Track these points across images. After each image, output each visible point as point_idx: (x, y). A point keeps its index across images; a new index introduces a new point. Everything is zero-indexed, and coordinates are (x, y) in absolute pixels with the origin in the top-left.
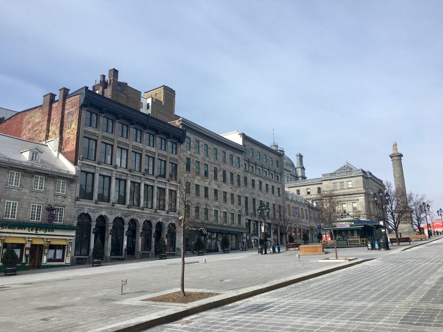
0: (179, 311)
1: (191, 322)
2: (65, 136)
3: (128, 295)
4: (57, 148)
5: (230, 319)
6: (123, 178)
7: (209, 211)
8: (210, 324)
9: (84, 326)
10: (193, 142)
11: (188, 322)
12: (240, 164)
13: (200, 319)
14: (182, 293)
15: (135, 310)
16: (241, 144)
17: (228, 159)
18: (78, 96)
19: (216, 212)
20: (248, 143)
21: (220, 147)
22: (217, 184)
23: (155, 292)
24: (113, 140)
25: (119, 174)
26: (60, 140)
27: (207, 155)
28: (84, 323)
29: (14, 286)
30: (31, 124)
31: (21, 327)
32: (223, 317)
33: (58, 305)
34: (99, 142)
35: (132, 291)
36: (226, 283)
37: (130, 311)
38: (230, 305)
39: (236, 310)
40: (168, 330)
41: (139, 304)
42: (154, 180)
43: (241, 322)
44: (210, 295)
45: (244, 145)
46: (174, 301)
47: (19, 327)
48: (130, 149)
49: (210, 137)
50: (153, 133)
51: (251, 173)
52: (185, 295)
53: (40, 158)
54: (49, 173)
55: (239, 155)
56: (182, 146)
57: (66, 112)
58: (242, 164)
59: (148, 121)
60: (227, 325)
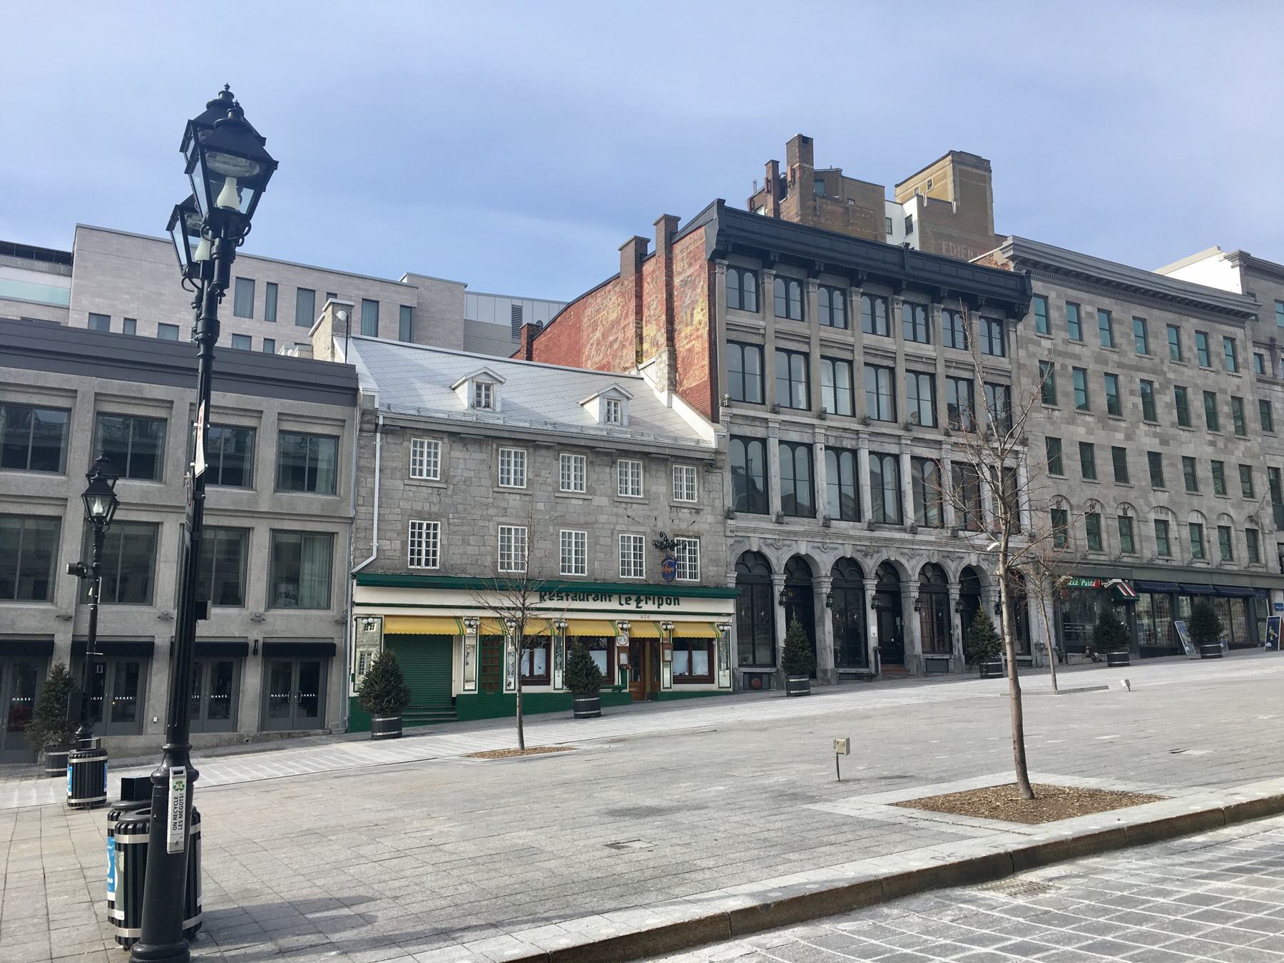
0: (1001, 850)
1: (1043, 889)
2: (682, 345)
3: (857, 787)
4: (666, 383)
5: (1188, 891)
6: (848, 444)
7: (1135, 524)
8: (1112, 902)
9: (708, 874)
10: (1059, 308)
11: (1033, 889)
12: (1240, 360)
13: (1081, 881)
14: (1022, 790)
15: (865, 833)
16: (1240, 292)
17: (1190, 349)
18: (702, 230)
19: (1162, 525)
20: (1263, 285)
21: (1156, 312)
22: (1155, 435)
23: (940, 780)
24: (806, 340)
25: (834, 433)
26: (669, 358)
27: (1113, 345)
28: (711, 863)
29: (585, 747)
30: (600, 328)
31: (552, 864)
32: (1163, 881)
33: (664, 804)
34: (769, 349)
35: (871, 773)
36: (1189, 760)
37: (850, 836)
38: (1199, 839)
39: (1221, 859)
40: (961, 909)
41: (880, 817)
42: (940, 443)
43: (1230, 907)
44: (1125, 801)
45: (1249, 293)
46: (994, 813)
47: (547, 865)
48: (859, 358)
49: (1119, 284)
50: (923, 299)
52: (1032, 797)
53: (498, 398)
54: (652, 450)
55: (1232, 329)
56: (1020, 326)
57: (677, 281)
58: (1246, 360)
59: (903, 267)
60: (1177, 910)
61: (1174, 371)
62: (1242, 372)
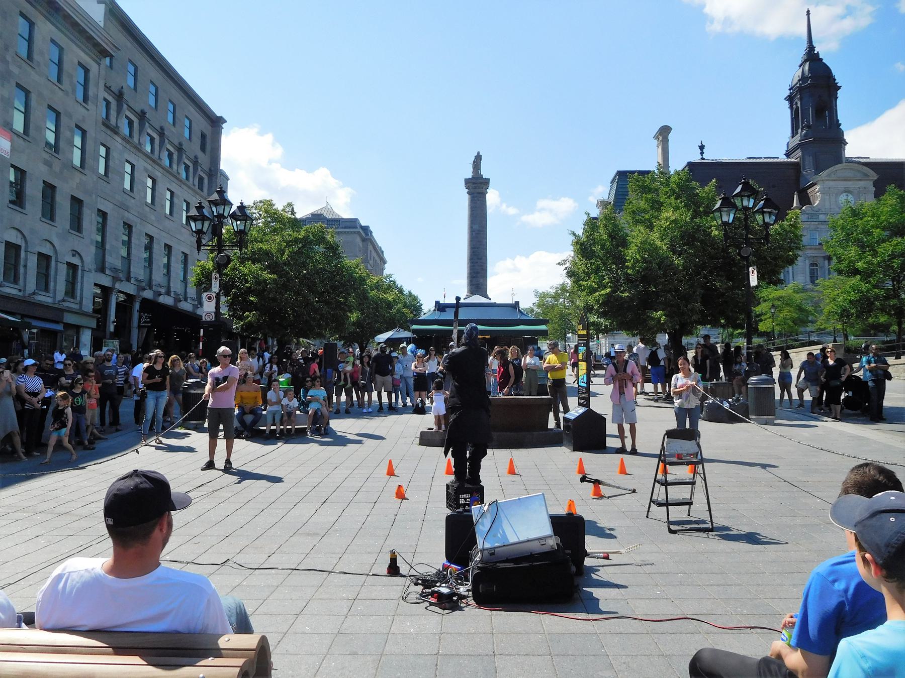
12: (91, 93)
51: (127, 142)
61: (20, 67)
62: (90, 106)
